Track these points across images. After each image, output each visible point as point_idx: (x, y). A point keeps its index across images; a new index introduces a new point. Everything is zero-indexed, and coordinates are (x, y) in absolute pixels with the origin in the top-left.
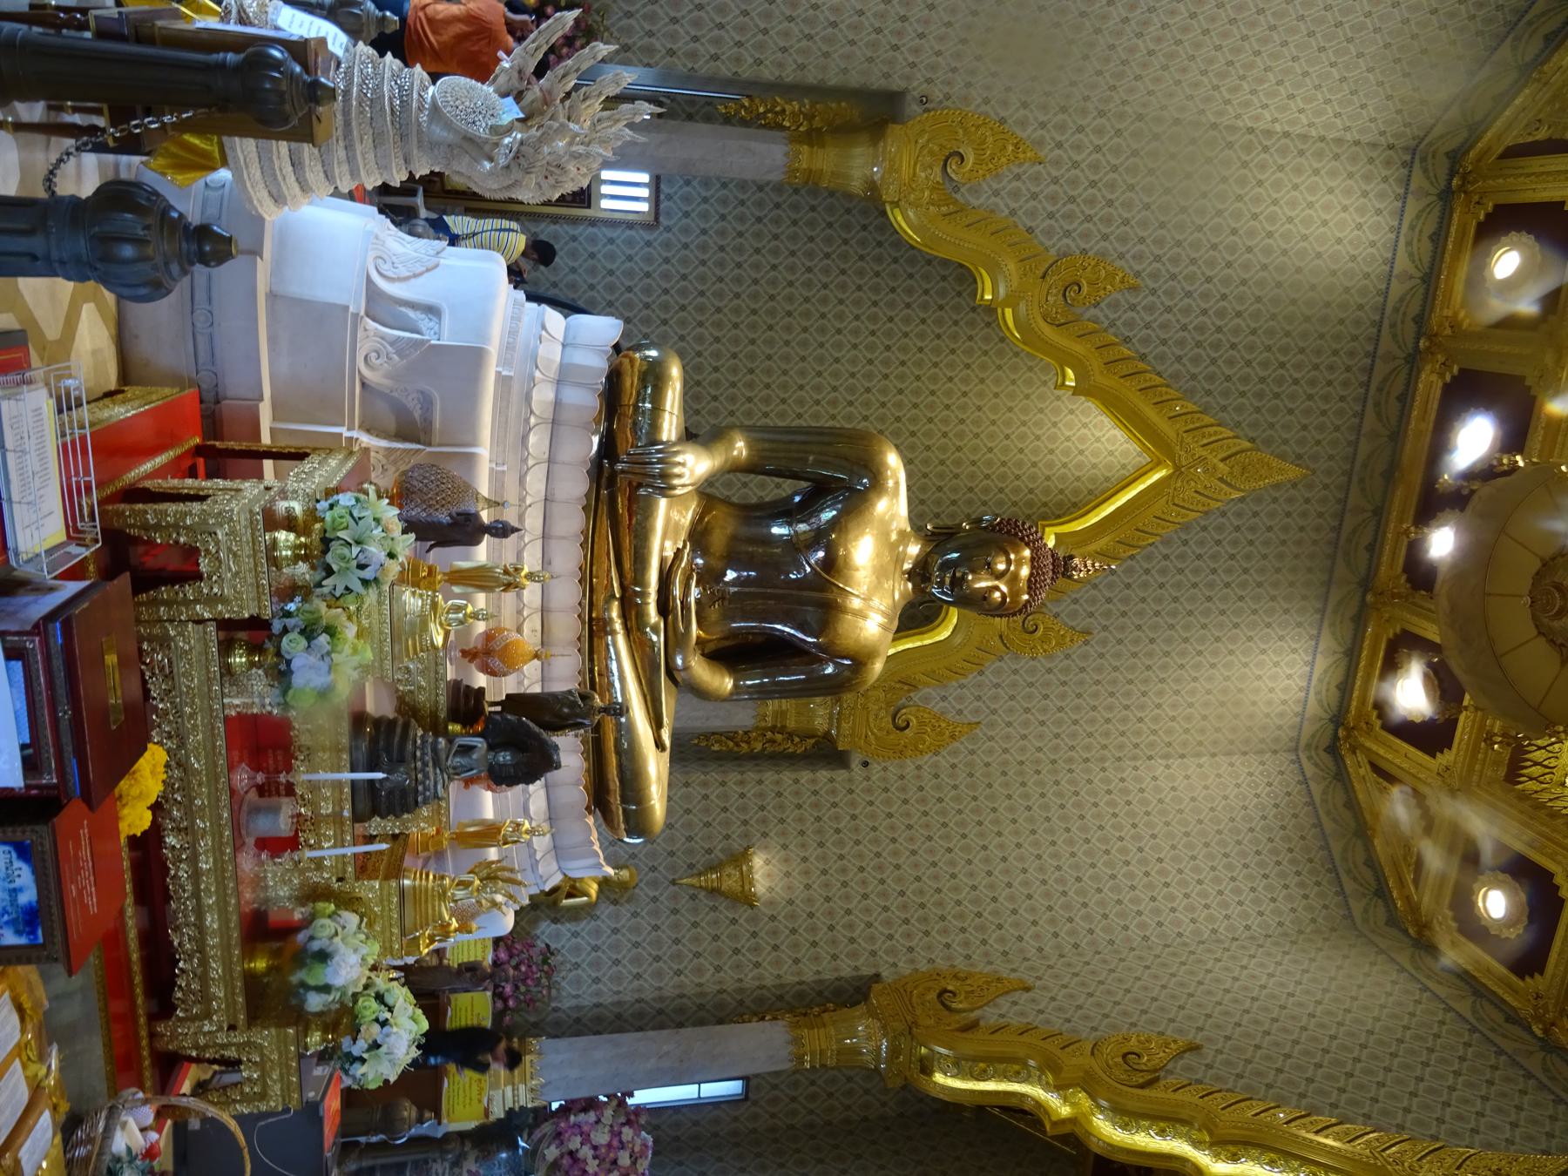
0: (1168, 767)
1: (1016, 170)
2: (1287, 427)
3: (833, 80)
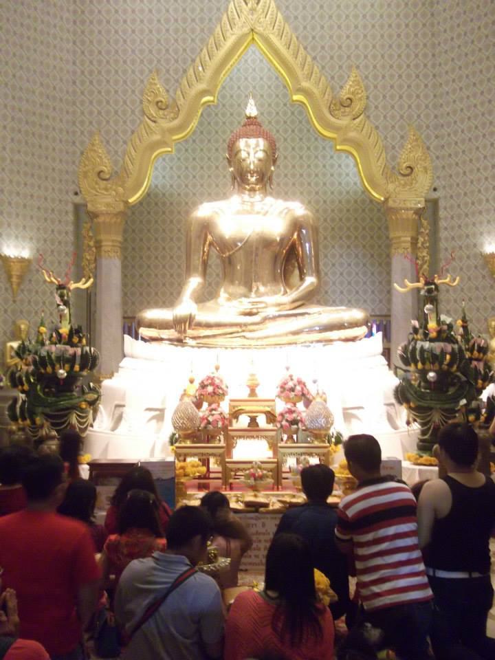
3: (71, 238)
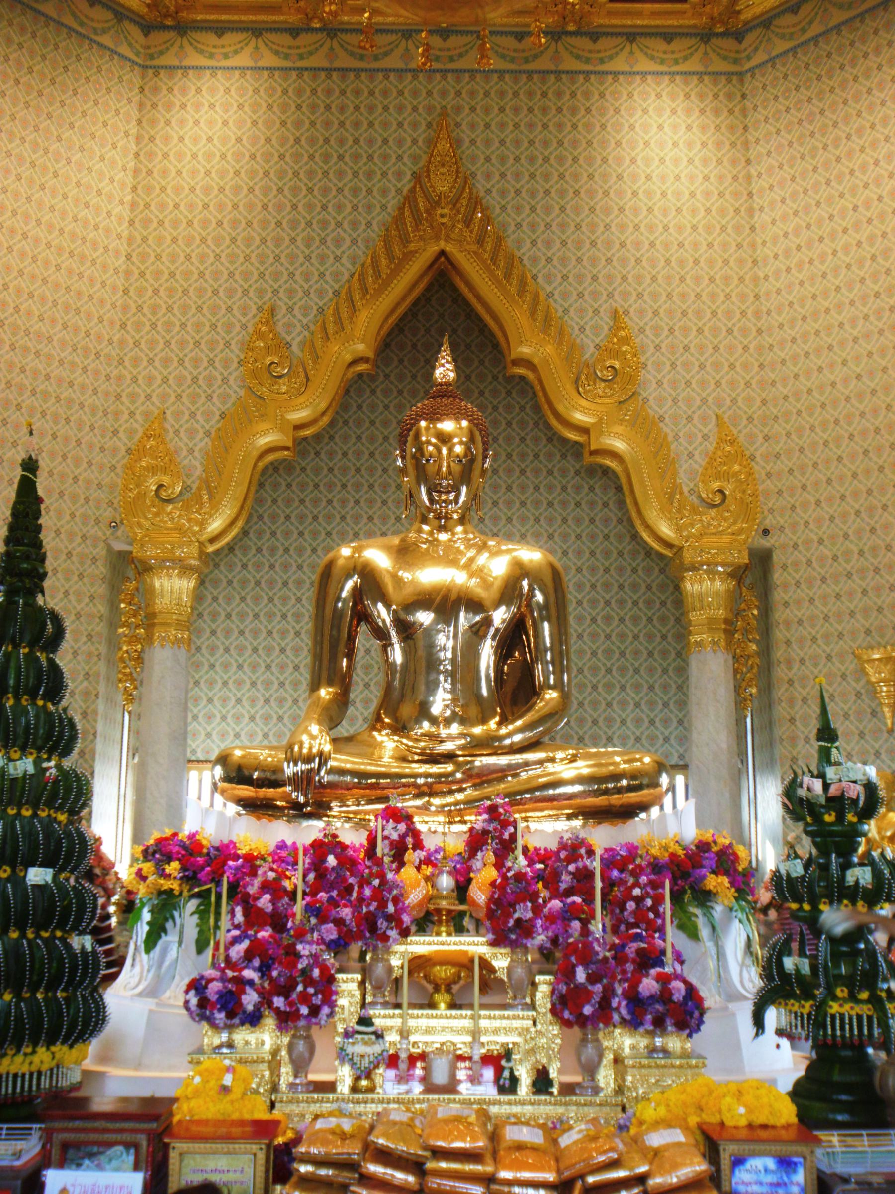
0: (761, 209)
1: (171, 434)
2: (400, 142)
3: (102, 608)
